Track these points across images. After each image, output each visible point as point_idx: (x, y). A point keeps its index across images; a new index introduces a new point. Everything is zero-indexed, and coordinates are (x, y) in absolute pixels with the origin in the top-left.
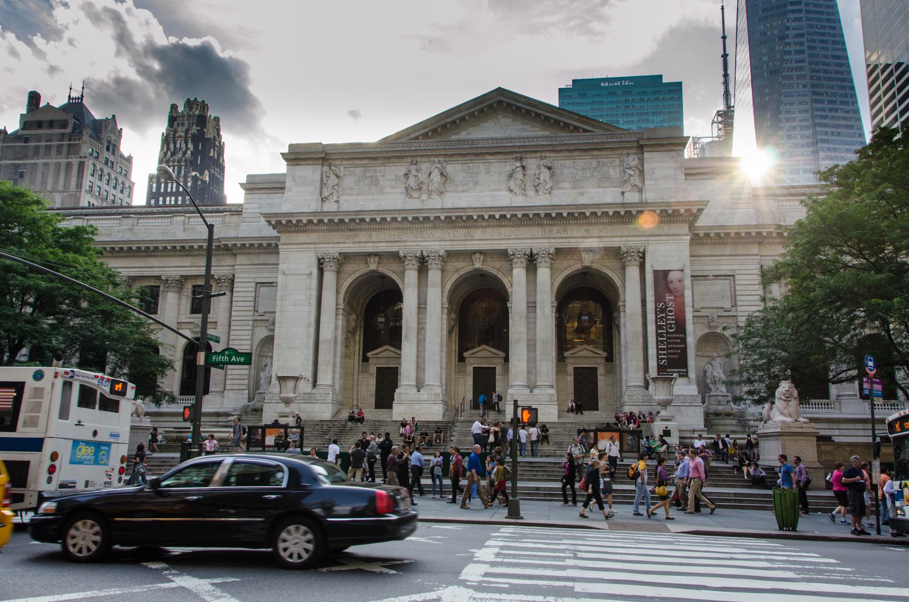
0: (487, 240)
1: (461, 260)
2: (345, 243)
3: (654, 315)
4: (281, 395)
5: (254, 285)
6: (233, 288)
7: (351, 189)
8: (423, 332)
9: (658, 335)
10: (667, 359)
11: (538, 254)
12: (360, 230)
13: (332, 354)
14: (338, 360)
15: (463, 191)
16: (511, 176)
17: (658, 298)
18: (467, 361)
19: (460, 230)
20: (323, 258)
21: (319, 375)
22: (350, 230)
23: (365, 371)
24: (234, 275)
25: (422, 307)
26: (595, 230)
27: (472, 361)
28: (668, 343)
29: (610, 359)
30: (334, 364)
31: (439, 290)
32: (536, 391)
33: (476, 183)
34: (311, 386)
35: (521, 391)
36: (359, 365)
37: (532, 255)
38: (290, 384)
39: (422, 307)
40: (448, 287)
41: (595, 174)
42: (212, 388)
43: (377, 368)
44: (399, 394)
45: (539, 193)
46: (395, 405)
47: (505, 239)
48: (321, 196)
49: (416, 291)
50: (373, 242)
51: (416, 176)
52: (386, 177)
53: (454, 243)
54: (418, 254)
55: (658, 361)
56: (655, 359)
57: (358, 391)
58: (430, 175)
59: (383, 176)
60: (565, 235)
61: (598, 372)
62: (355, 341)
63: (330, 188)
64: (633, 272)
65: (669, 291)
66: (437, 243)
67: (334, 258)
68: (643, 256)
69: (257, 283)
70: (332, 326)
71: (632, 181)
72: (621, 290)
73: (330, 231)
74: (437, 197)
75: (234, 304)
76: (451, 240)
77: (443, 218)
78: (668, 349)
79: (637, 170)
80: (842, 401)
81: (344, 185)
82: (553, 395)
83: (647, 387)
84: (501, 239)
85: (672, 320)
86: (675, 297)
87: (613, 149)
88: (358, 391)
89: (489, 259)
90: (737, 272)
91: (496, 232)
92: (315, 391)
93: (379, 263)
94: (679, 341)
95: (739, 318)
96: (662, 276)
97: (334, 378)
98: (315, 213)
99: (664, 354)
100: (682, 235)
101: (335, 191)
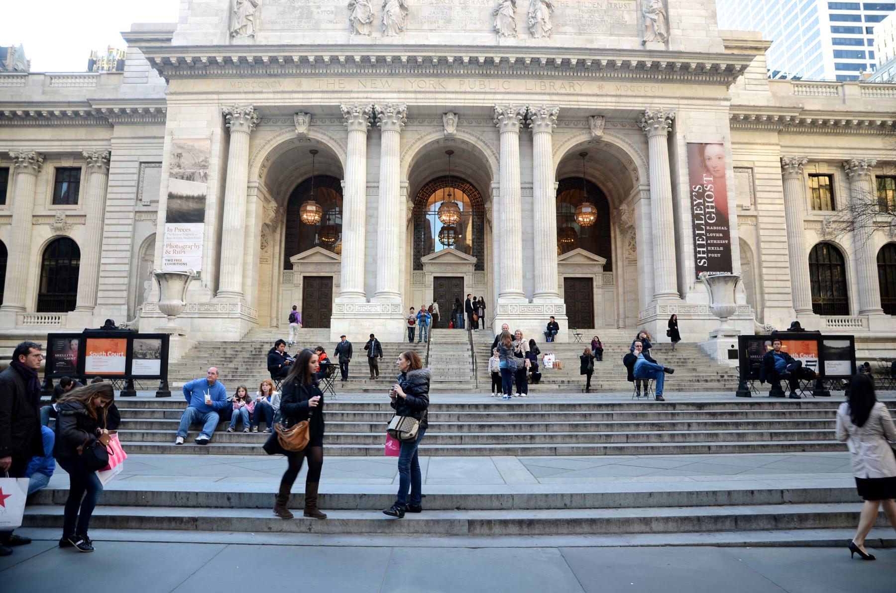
0: (465, 93)
1: (426, 123)
2: (261, 92)
3: (689, 200)
4: (161, 303)
5: (137, 164)
6: (108, 170)
7: (273, 23)
8: (373, 220)
9: (696, 227)
10: (708, 259)
11: (535, 114)
12: (285, 75)
13: (242, 249)
14: (250, 259)
15: (431, 30)
16: (496, 13)
17: (694, 179)
18: (426, 268)
19: (427, 80)
20: (230, 114)
21: (222, 279)
22: (270, 76)
23: (288, 281)
24: (110, 153)
25: (372, 186)
27: (432, 268)
28: (708, 238)
29: (608, 268)
30: (245, 264)
31: (396, 160)
32: (536, 301)
33: (449, 21)
34: (210, 293)
35: (516, 301)
36: (279, 273)
37: (526, 117)
38: (176, 285)
39: (372, 186)
40: (409, 159)
41: (606, 18)
42: (79, 302)
43: (305, 277)
44: (338, 305)
45: (536, 36)
46: (333, 322)
47: (490, 93)
48: (229, 28)
49: (364, 160)
50: (303, 92)
51: (365, 5)
52: (323, 9)
53: (419, 96)
54: (368, 109)
55: (696, 262)
56: (693, 258)
57: (278, 307)
58: (384, 6)
59: (319, 7)
60: (572, 91)
61: (595, 284)
62: (274, 240)
63: (243, 18)
64: (659, 144)
65: (707, 170)
67: (246, 114)
68: (672, 123)
69: (141, 163)
70: (242, 209)
71: (656, 28)
72: (641, 172)
73: (242, 76)
74: (394, 34)
75: (109, 189)
76: (415, 92)
77: (404, 59)
78: (708, 245)
79: (661, 14)
80: (870, 317)
81: (262, 17)
82: (560, 306)
83: (681, 294)
84: (486, 93)
85: (712, 207)
86: (714, 177)
88: (278, 307)
89: (465, 124)
90: (757, 164)
92: (216, 300)
93: (310, 125)
94: (721, 235)
95: (760, 219)
96: (697, 150)
97: (243, 285)
98: (218, 48)
99: (704, 252)
100: (720, 100)
101: (249, 23)
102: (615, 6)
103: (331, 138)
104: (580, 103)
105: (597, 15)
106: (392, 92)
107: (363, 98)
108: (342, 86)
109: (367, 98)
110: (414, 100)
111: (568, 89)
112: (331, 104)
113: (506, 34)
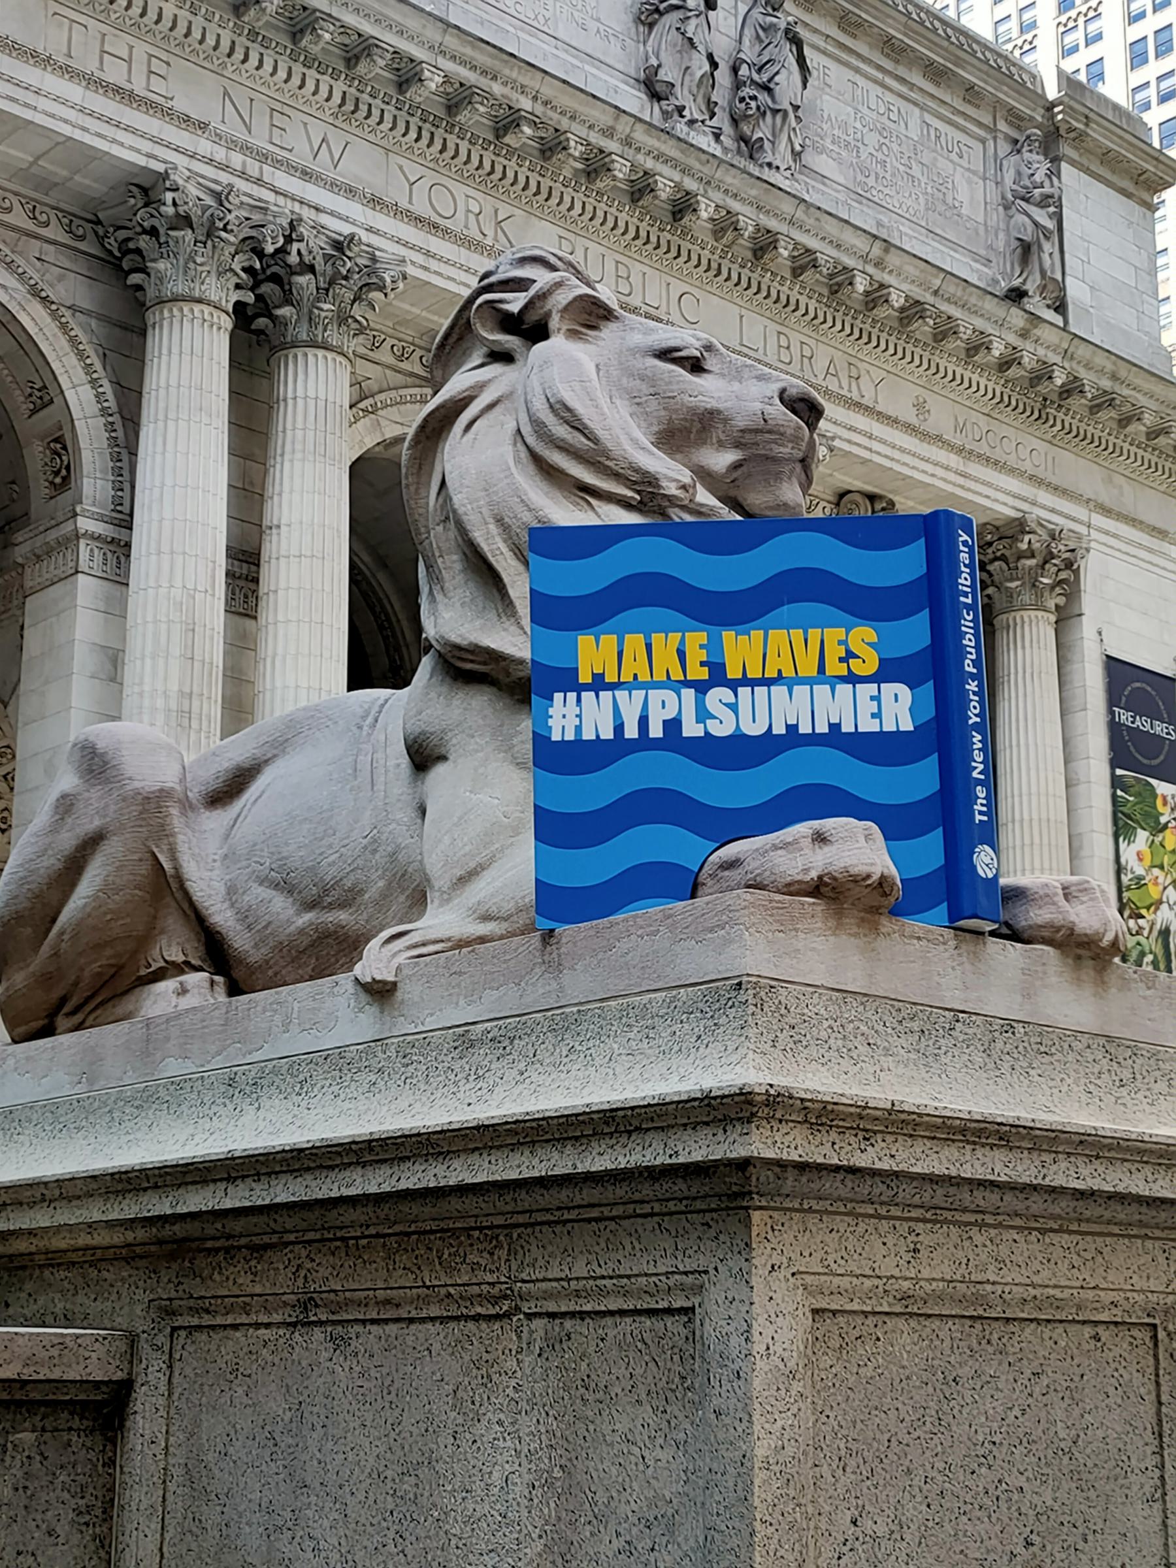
19: (460, 190)
26: (941, 418)
41: (916, 170)
53: (436, 244)
60: (855, 395)
66: (355, 209)
87: (971, 93)
91: (610, 266)
102: (938, 137)
103: (35, 292)
104: (876, 446)
105: (895, 146)
106: (350, 192)
107: (243, 175)
108: (157, 85)
109: (259, 181)
110: (419, 259)
111: (845, 384)
112: (116, 151)
113: (686, 113)
